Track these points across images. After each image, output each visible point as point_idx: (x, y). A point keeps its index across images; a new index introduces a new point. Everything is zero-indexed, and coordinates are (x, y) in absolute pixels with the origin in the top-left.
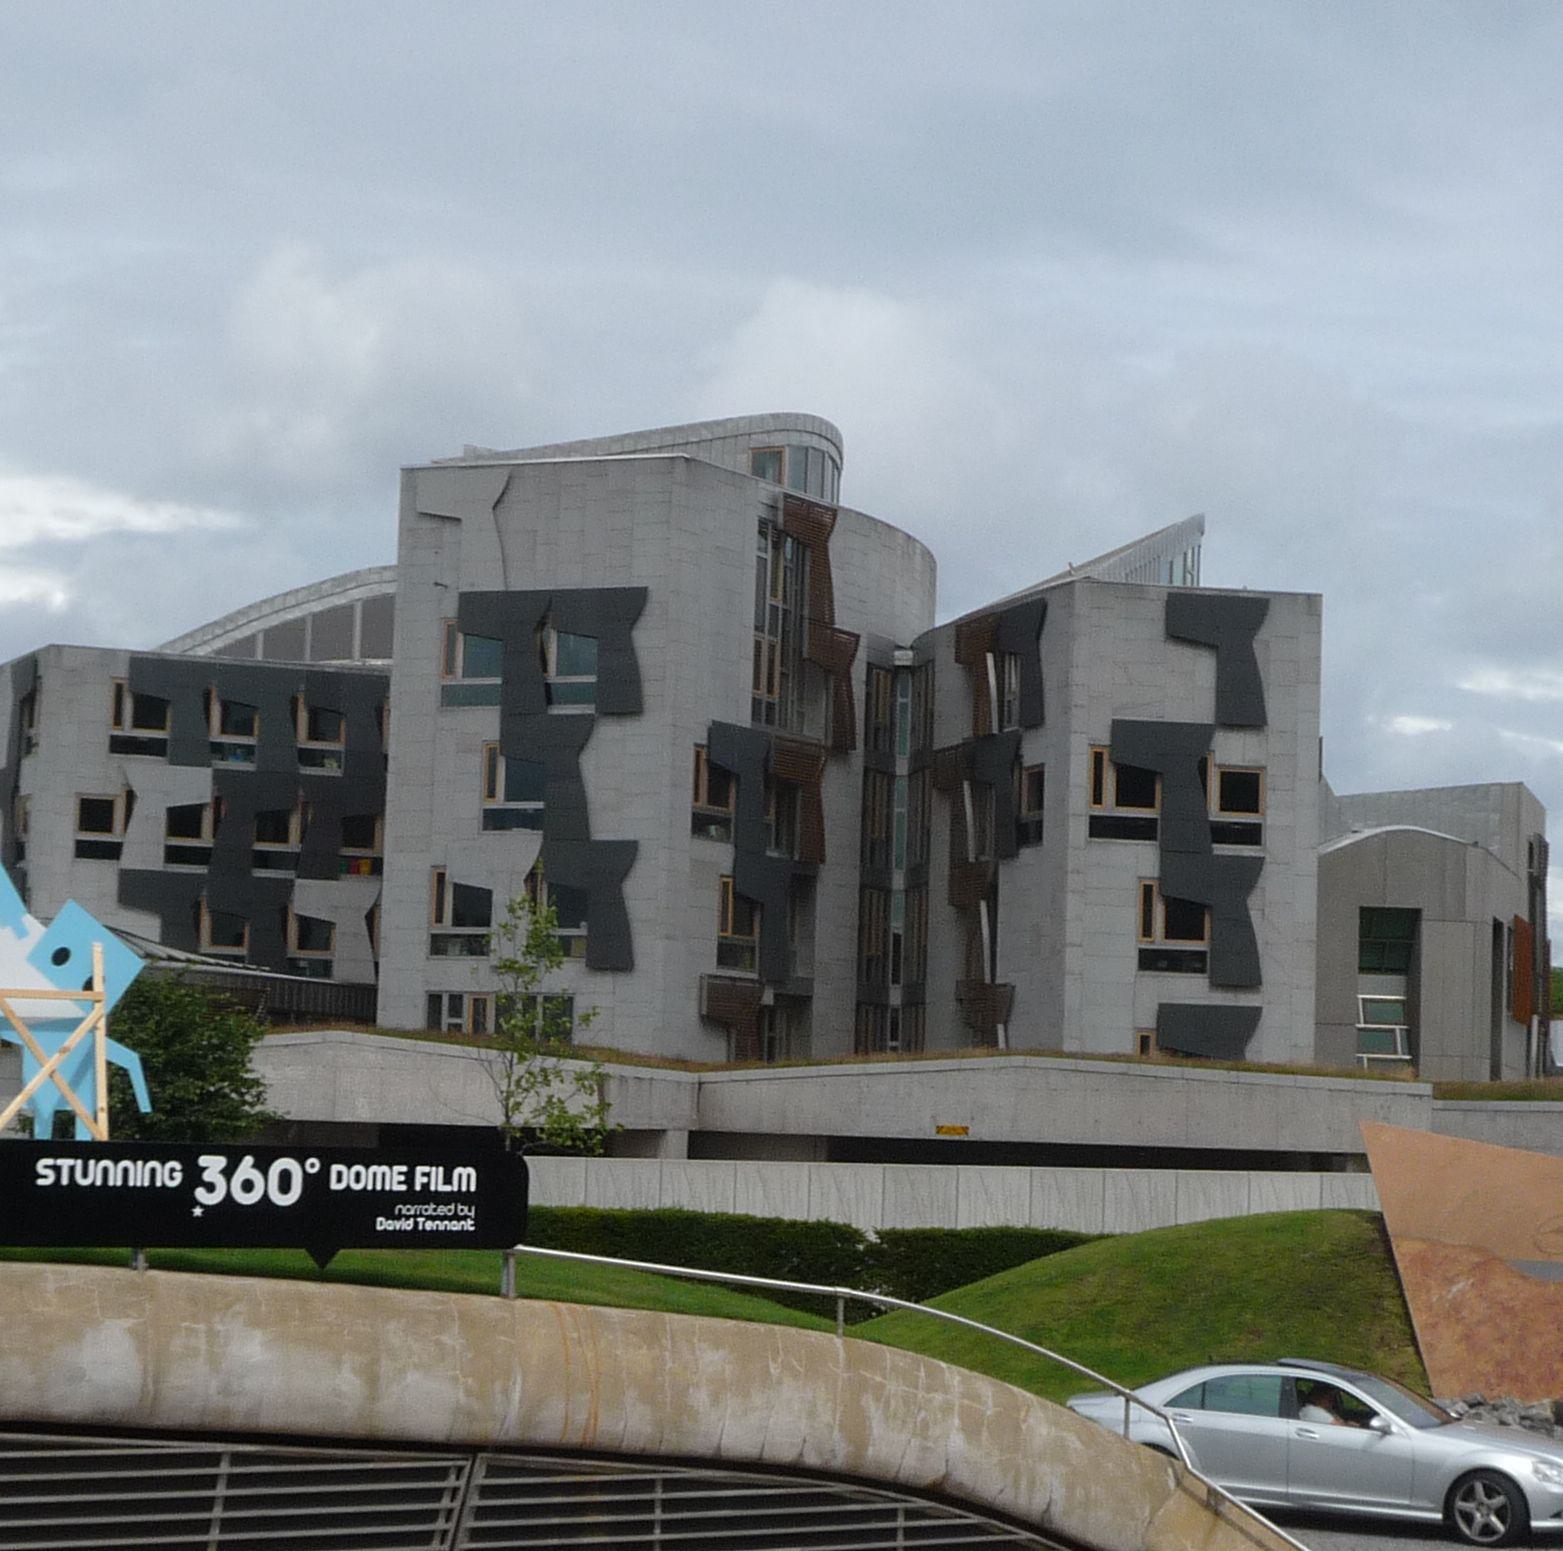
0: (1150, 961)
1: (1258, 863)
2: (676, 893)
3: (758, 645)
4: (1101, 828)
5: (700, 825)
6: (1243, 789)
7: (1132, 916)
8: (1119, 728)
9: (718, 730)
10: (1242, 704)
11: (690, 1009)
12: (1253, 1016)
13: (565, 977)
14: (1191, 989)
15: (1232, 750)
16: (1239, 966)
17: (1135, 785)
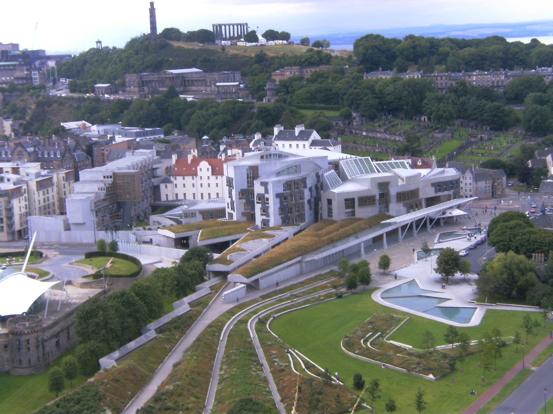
0: (262, 215)
1: (268, 207)
2: (239, 205)
3: (248, 181)
4: (257, 203)
5: (240, 199)
6: (267, 199)
7: (259, 211)
8: (258, 194)
9: (241, 190)
10: (267, 191)
11: (241, 215)
12: (269, 221)
13: (232, 212)
14: (264, 217)
15: (266, 196)
16: (268, 215)
17: (259, 199)
